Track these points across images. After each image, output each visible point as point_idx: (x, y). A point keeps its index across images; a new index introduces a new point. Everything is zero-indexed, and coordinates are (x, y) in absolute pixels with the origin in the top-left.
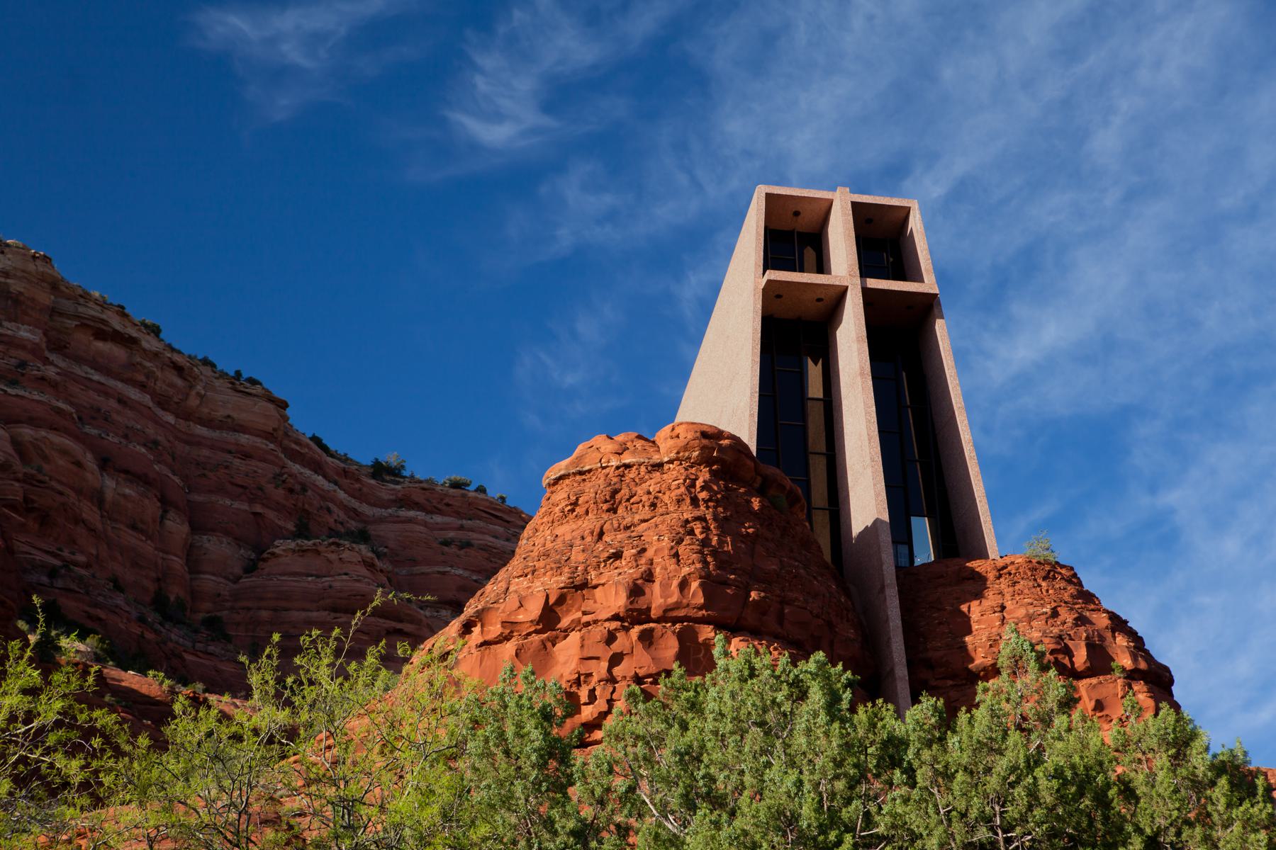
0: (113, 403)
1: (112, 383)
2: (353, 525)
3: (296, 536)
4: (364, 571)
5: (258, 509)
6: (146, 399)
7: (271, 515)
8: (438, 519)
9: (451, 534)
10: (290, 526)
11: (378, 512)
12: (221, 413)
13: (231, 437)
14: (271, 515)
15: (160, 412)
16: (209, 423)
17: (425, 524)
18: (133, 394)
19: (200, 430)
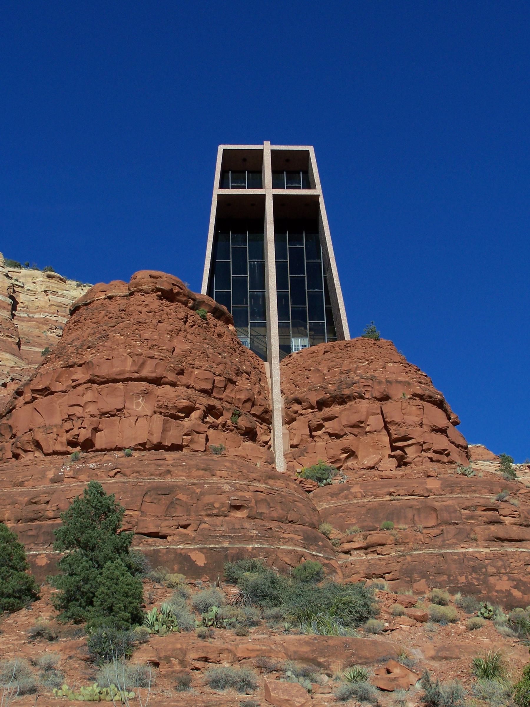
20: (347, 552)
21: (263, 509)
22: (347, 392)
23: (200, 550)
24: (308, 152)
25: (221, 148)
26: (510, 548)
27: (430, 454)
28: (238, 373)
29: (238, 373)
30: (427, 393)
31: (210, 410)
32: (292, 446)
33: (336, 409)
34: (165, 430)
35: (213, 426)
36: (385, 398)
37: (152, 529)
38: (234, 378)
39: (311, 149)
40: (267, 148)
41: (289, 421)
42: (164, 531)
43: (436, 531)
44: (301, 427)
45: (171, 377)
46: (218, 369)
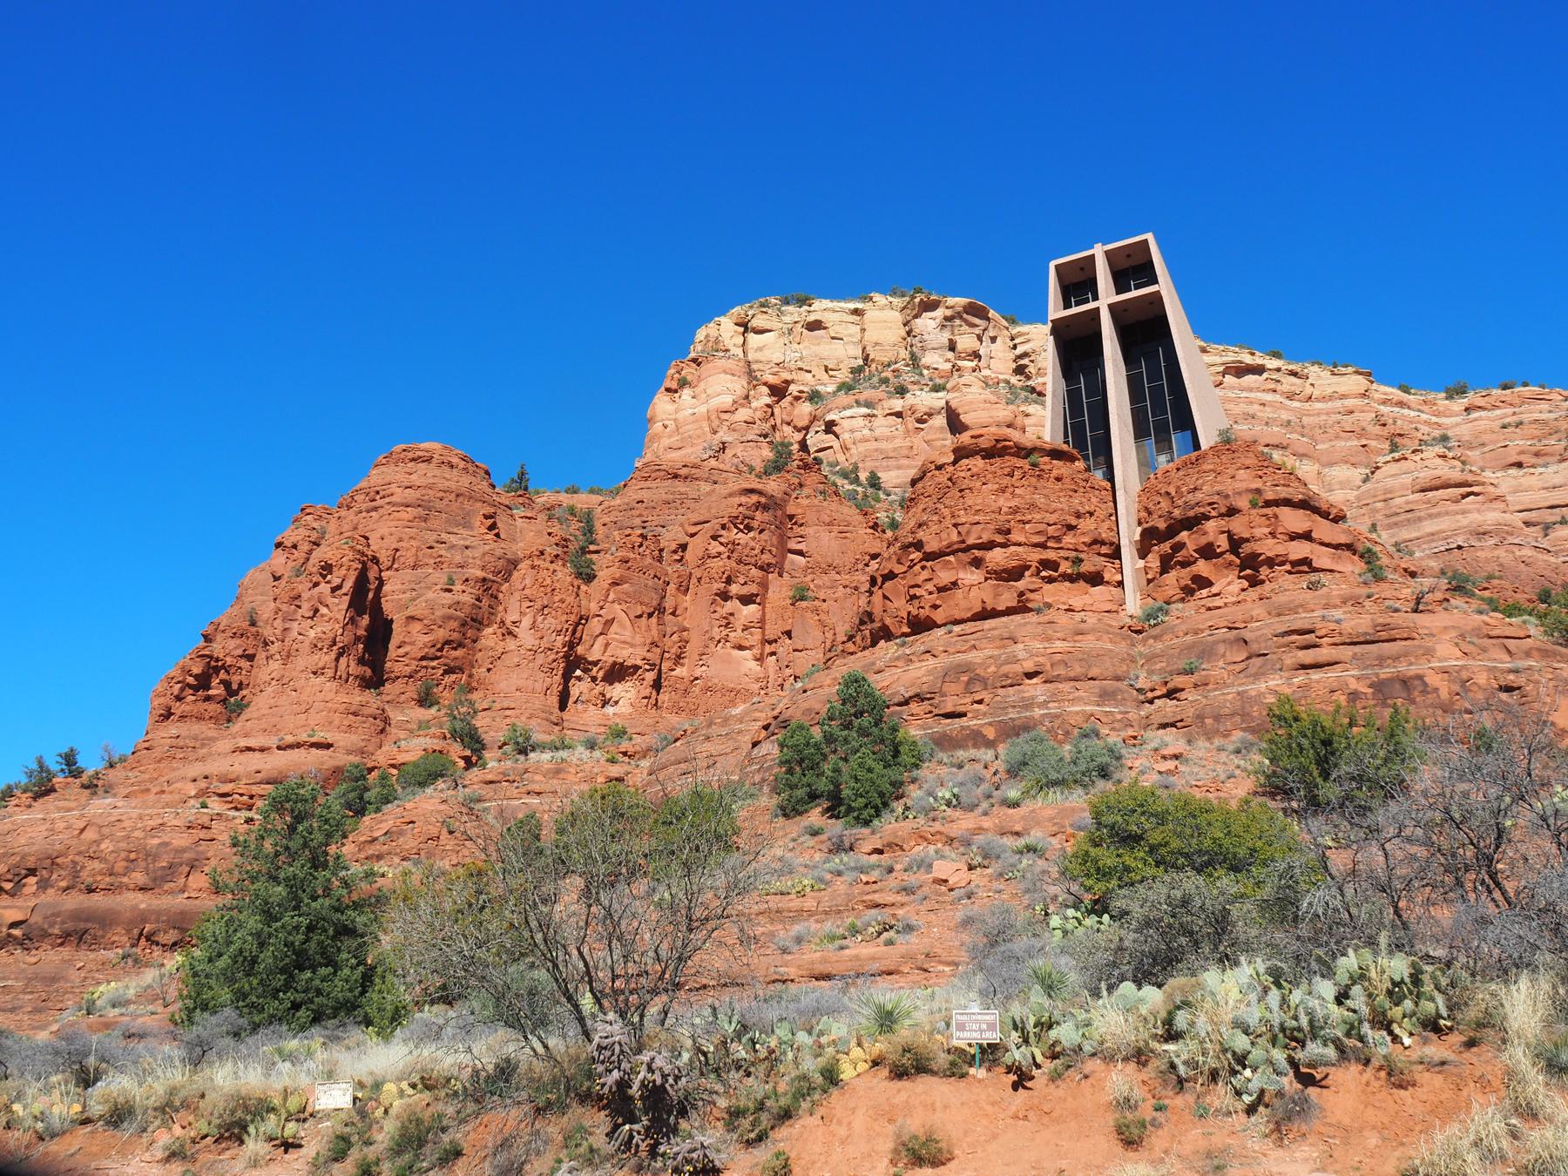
0: (1256, 407)
1: (1252, 395)
2: (1437, 433)
3: (1392, 451)
4: (1439, 461)
5: (1364, 442)
6: (1278, 397)
7: (1373, 443)
8: (1498, 412)
9: (1507, 420)
10: (1386, 446)
11: (1453, 420)
12: (1329, 391)
13: (1338, 404)
14: (1373, 443)
15: (1288, 402)
16: (1323, 399)
17: (1489, 419)
18: (1269, 397)
19: (1319, 405)
20: (1151, 702)
21: (1061, 671)
22: (1191, 513)
23: (990, 724)
24: (1146, 241)
25: (1052, 264)
26: (1315, 675)
27: (1288, 567)
28: (1078, 515)
29: (1078, 515)
30: (1283, 495)
31: (1046, 564)
32: (1149, 581)
33: (1184, 535)
34: (997, 595)
35: (1050, 580)
36: (1232, 512)
37: (949, 709)
38: (1074, 522)
39: (1149, 237)
40: (1099, 251)
41: (1143, 553)
42: (961, 709)
43: (1242, 666)
44: (1154, 561)
45: (1000, 539)
46: (1052, 518)
